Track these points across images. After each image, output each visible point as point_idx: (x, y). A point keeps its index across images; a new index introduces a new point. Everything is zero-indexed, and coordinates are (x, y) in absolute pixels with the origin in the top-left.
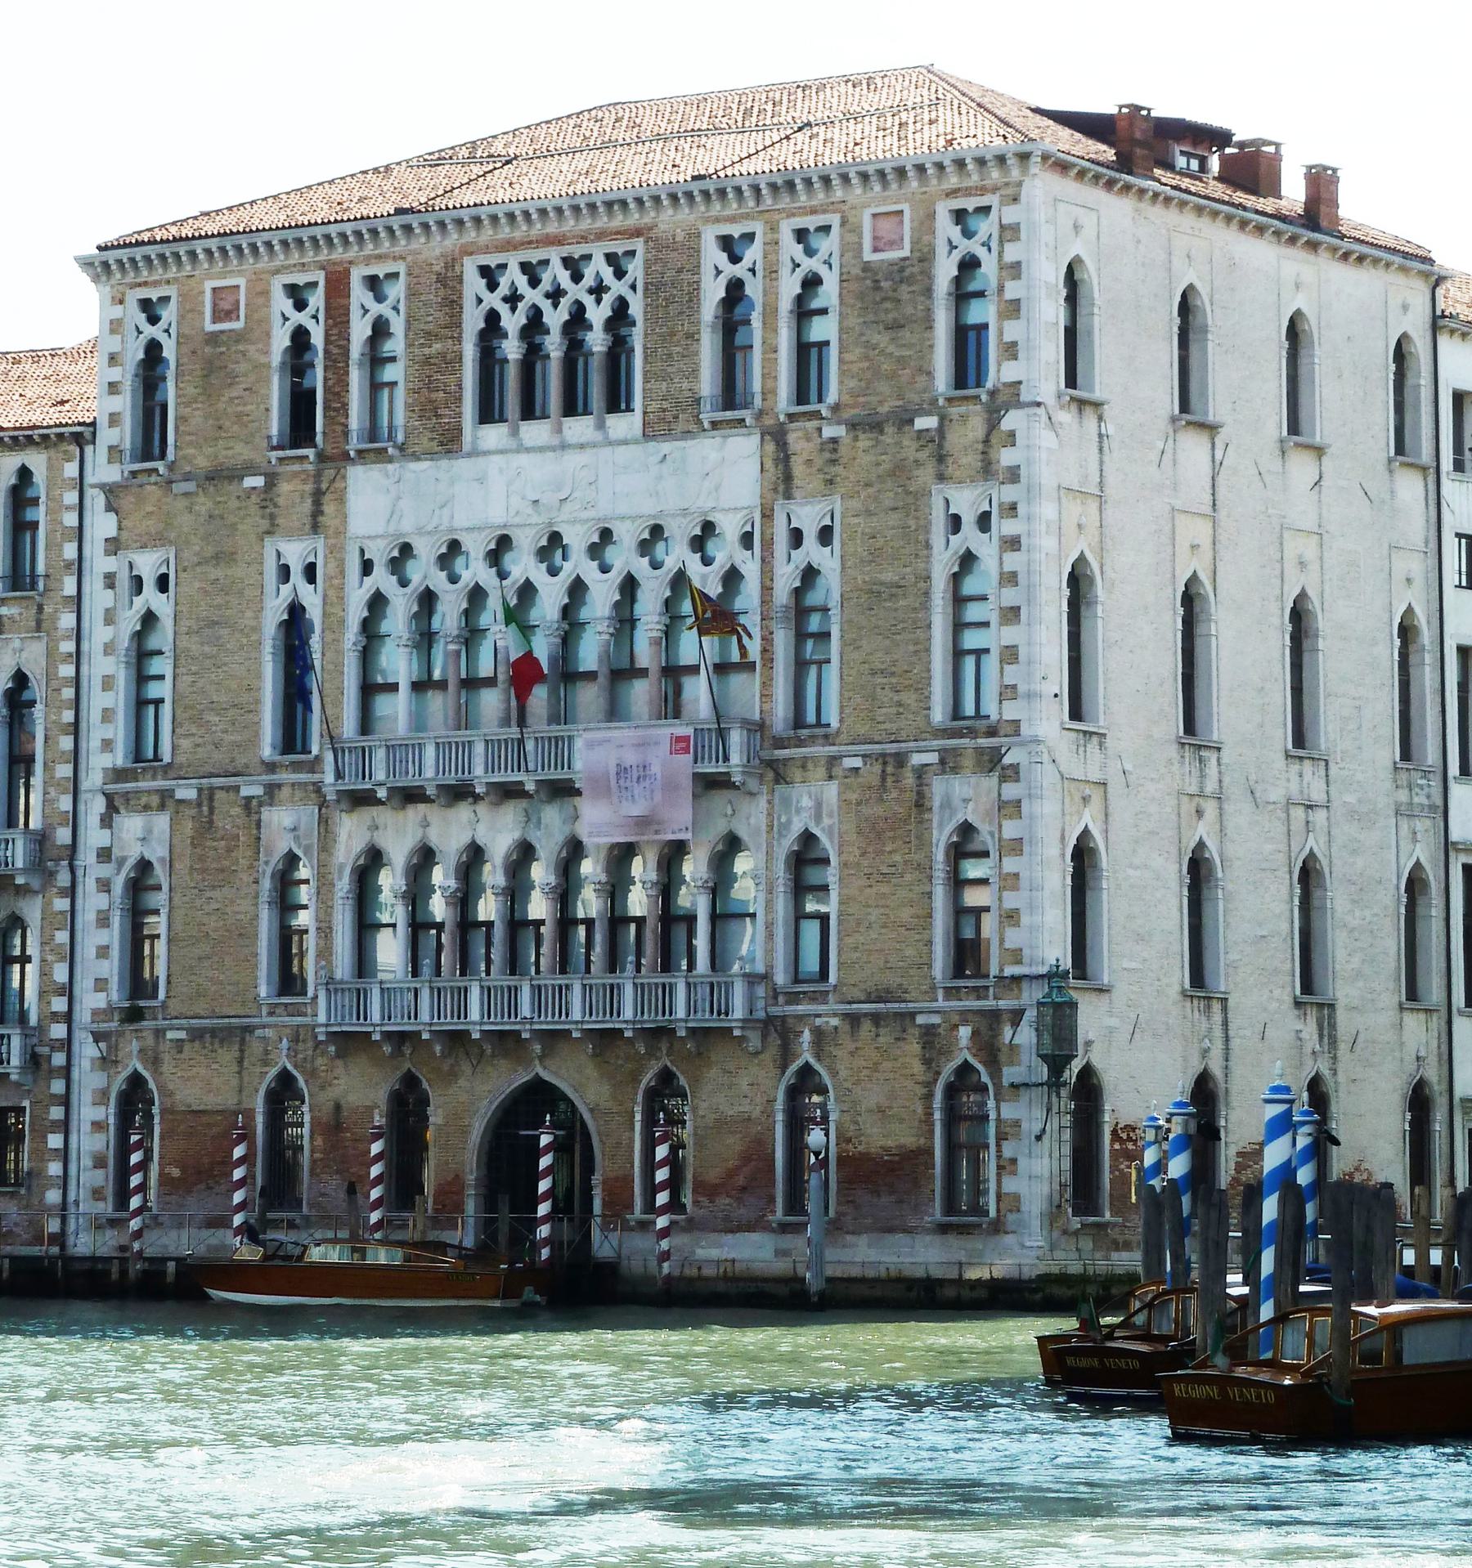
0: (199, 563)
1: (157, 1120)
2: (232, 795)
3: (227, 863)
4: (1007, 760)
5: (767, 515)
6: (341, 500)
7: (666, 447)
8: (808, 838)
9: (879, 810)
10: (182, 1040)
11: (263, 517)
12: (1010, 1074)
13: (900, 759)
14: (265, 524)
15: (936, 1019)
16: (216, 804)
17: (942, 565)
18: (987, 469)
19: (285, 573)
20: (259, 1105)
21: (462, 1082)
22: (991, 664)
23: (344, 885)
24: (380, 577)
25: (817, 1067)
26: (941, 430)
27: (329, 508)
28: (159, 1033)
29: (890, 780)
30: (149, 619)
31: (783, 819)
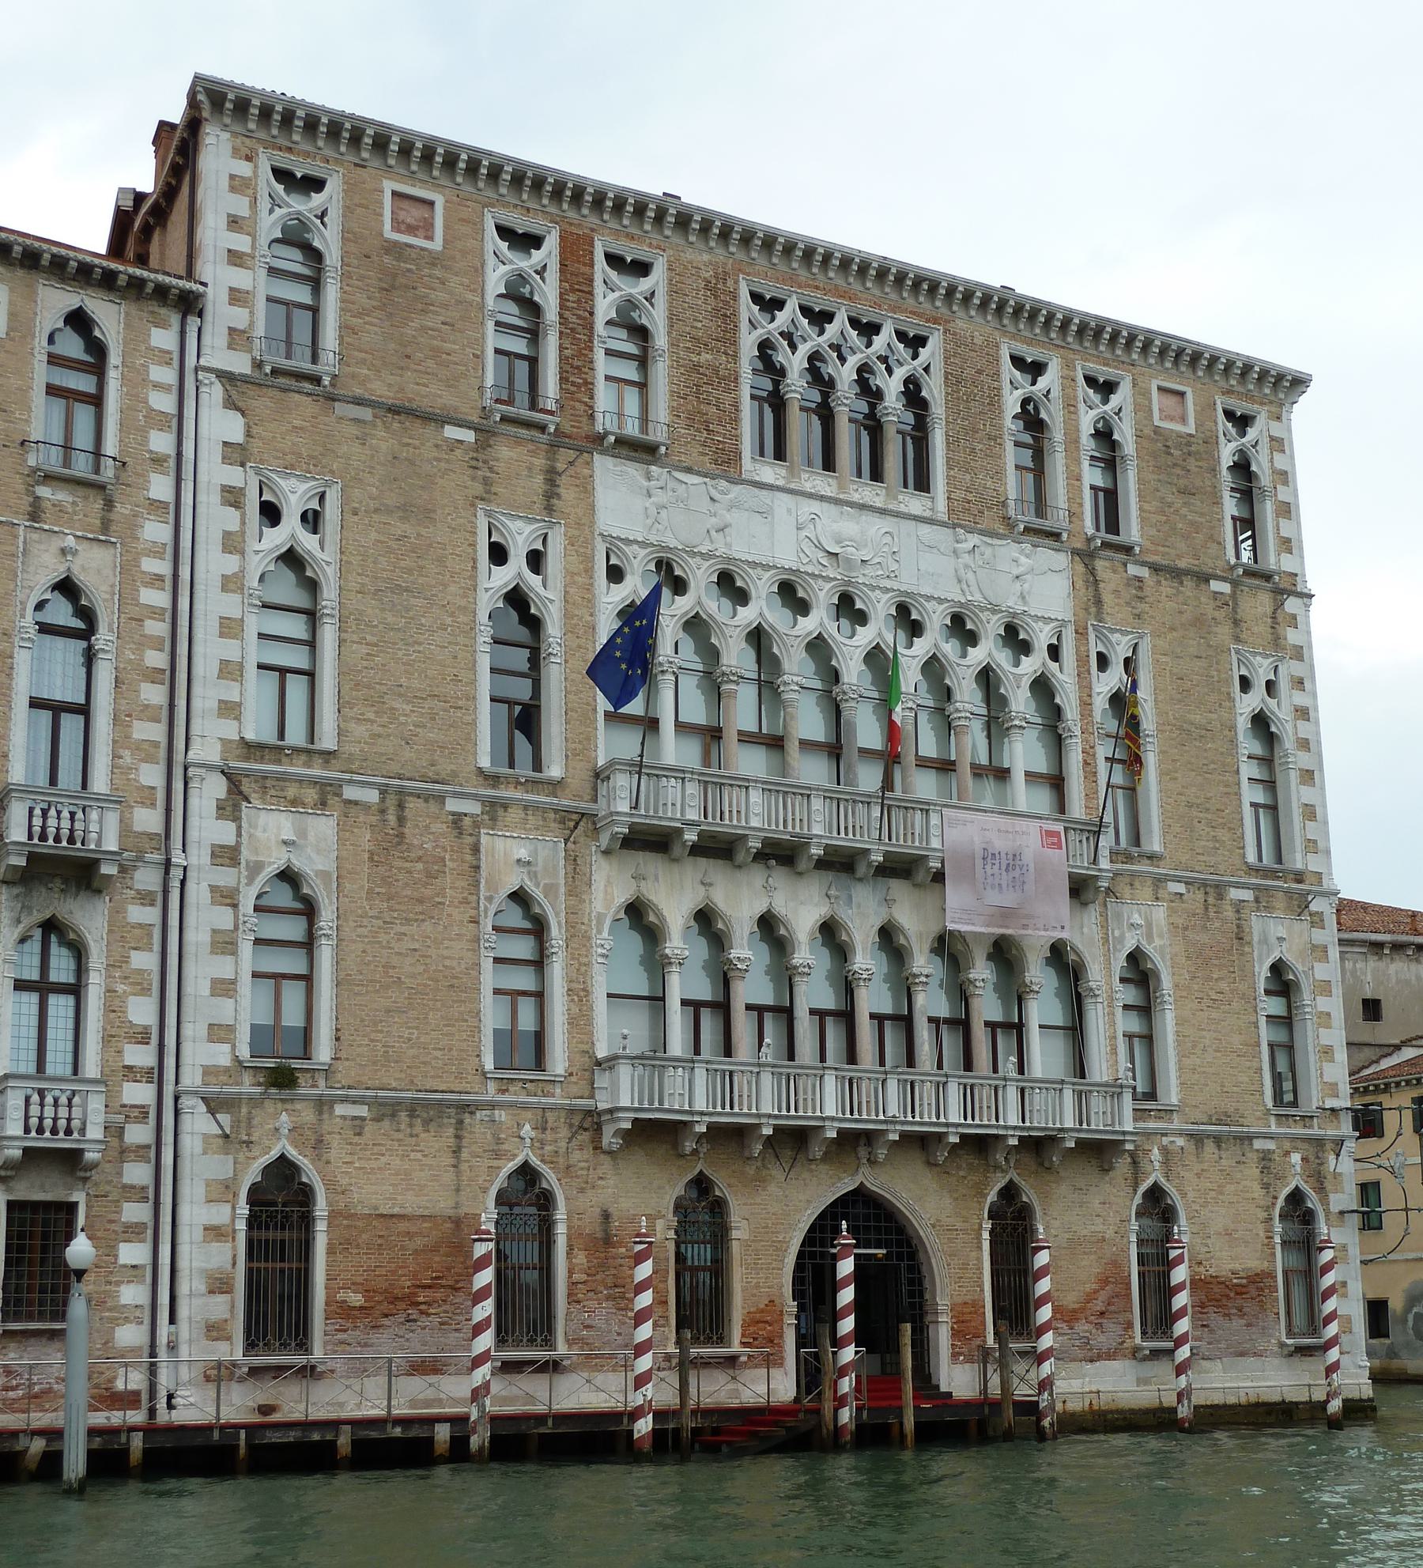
0: (376, 510)
1: (321, 1226)
2: (433, 807)
3: (428, 892)
4: (1313, 907)
5: (1081, 633)
6: (586, 488)
7: (974, 539)
9: (1204, 938)
10: (363, 1119)
11: (473, 479)
13: (1220, 889)
14: (479, 489)
15: (1271, 1145)
16: (407, 812)
18: (1276, 641)
19: (499, 555)
21: (772, 1188)
25: (1167, 1186)
26: (1233, 595)
27: (567, 492)
29: (1211, 910)
31: (1117, 933)
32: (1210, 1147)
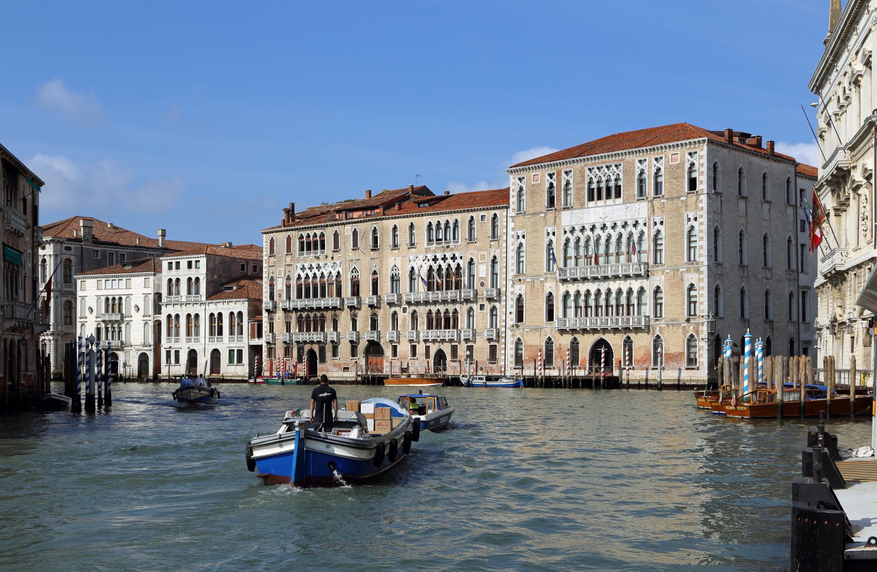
5: (649, 219)
6: (560, 218)
8: (658, 287)
12: (701, 336)
17: (686, 228)
18: (696, 208)
19: (548, 234)
20: (544, 344)
22: (697, 250)
23: (561, 298)
24: (569, 235)
30: (521, 244)
32: (671, 327)
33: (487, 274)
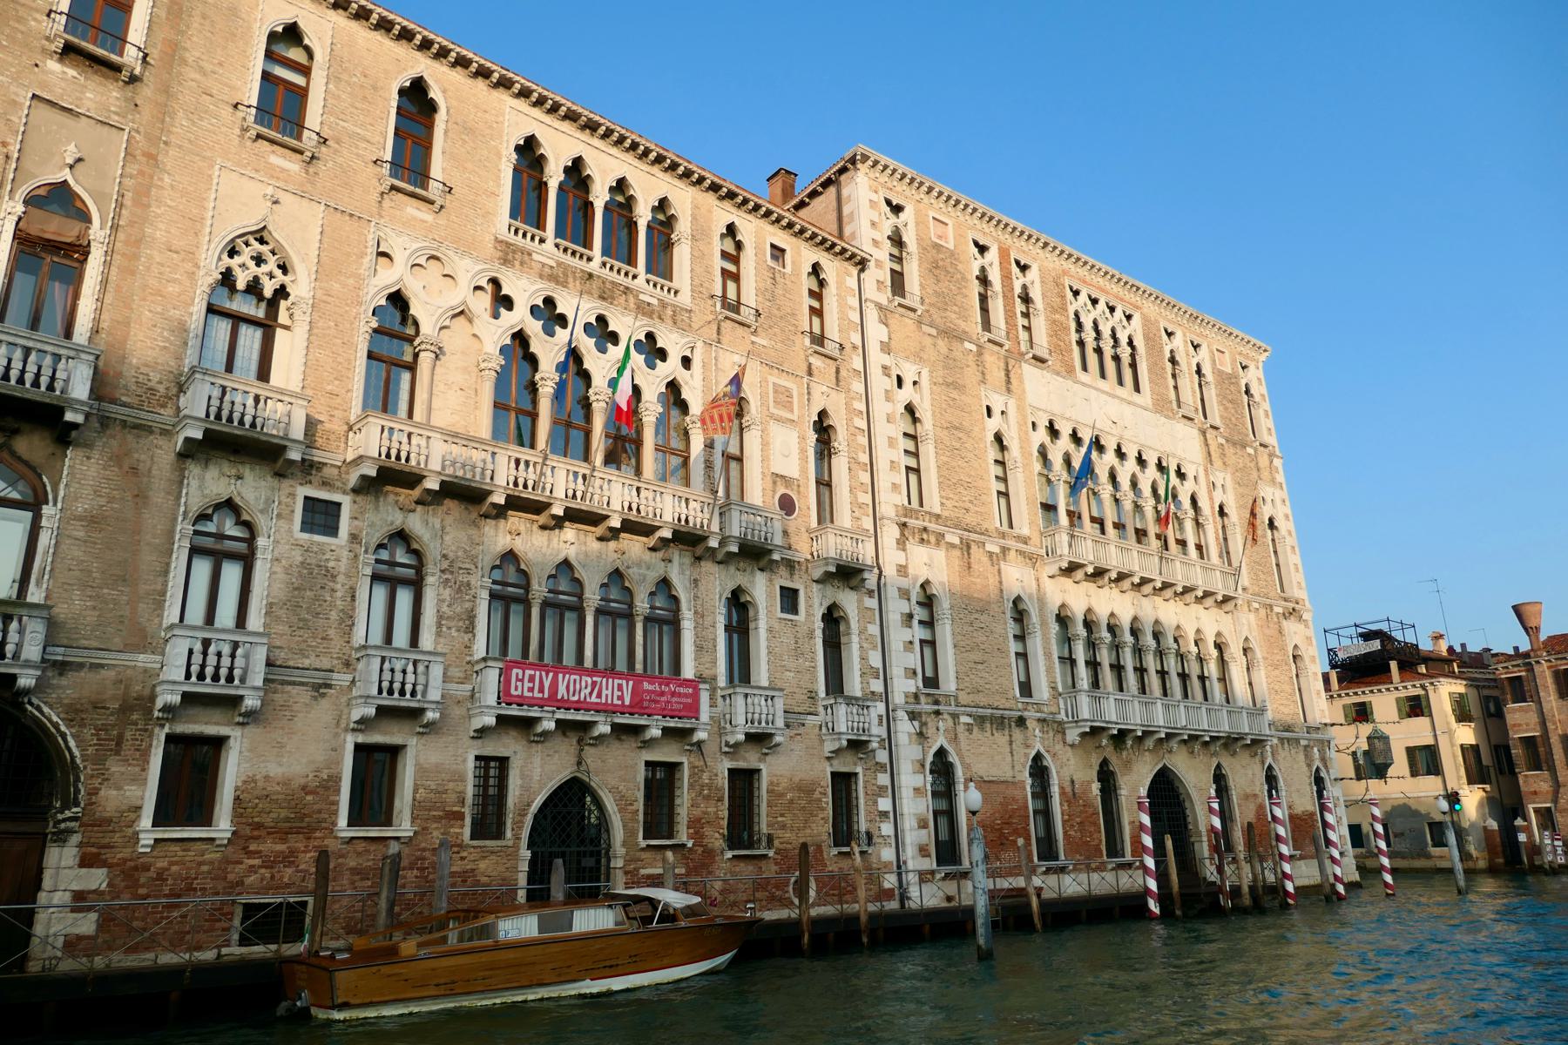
14: (980, 377)
28: (955, 716)
33: (804, 470)
